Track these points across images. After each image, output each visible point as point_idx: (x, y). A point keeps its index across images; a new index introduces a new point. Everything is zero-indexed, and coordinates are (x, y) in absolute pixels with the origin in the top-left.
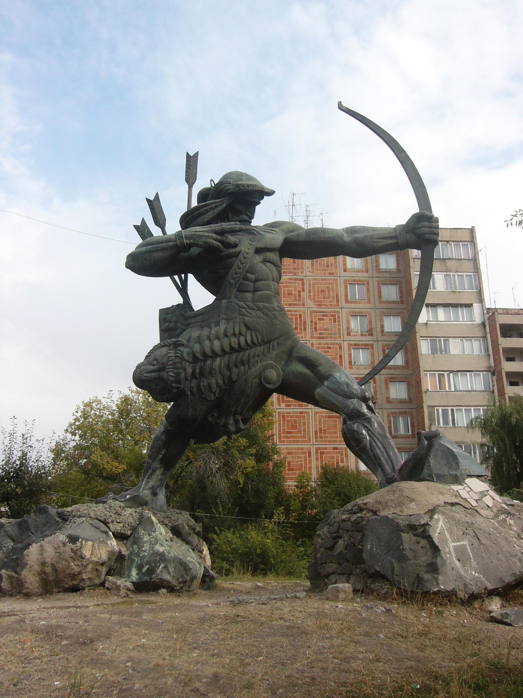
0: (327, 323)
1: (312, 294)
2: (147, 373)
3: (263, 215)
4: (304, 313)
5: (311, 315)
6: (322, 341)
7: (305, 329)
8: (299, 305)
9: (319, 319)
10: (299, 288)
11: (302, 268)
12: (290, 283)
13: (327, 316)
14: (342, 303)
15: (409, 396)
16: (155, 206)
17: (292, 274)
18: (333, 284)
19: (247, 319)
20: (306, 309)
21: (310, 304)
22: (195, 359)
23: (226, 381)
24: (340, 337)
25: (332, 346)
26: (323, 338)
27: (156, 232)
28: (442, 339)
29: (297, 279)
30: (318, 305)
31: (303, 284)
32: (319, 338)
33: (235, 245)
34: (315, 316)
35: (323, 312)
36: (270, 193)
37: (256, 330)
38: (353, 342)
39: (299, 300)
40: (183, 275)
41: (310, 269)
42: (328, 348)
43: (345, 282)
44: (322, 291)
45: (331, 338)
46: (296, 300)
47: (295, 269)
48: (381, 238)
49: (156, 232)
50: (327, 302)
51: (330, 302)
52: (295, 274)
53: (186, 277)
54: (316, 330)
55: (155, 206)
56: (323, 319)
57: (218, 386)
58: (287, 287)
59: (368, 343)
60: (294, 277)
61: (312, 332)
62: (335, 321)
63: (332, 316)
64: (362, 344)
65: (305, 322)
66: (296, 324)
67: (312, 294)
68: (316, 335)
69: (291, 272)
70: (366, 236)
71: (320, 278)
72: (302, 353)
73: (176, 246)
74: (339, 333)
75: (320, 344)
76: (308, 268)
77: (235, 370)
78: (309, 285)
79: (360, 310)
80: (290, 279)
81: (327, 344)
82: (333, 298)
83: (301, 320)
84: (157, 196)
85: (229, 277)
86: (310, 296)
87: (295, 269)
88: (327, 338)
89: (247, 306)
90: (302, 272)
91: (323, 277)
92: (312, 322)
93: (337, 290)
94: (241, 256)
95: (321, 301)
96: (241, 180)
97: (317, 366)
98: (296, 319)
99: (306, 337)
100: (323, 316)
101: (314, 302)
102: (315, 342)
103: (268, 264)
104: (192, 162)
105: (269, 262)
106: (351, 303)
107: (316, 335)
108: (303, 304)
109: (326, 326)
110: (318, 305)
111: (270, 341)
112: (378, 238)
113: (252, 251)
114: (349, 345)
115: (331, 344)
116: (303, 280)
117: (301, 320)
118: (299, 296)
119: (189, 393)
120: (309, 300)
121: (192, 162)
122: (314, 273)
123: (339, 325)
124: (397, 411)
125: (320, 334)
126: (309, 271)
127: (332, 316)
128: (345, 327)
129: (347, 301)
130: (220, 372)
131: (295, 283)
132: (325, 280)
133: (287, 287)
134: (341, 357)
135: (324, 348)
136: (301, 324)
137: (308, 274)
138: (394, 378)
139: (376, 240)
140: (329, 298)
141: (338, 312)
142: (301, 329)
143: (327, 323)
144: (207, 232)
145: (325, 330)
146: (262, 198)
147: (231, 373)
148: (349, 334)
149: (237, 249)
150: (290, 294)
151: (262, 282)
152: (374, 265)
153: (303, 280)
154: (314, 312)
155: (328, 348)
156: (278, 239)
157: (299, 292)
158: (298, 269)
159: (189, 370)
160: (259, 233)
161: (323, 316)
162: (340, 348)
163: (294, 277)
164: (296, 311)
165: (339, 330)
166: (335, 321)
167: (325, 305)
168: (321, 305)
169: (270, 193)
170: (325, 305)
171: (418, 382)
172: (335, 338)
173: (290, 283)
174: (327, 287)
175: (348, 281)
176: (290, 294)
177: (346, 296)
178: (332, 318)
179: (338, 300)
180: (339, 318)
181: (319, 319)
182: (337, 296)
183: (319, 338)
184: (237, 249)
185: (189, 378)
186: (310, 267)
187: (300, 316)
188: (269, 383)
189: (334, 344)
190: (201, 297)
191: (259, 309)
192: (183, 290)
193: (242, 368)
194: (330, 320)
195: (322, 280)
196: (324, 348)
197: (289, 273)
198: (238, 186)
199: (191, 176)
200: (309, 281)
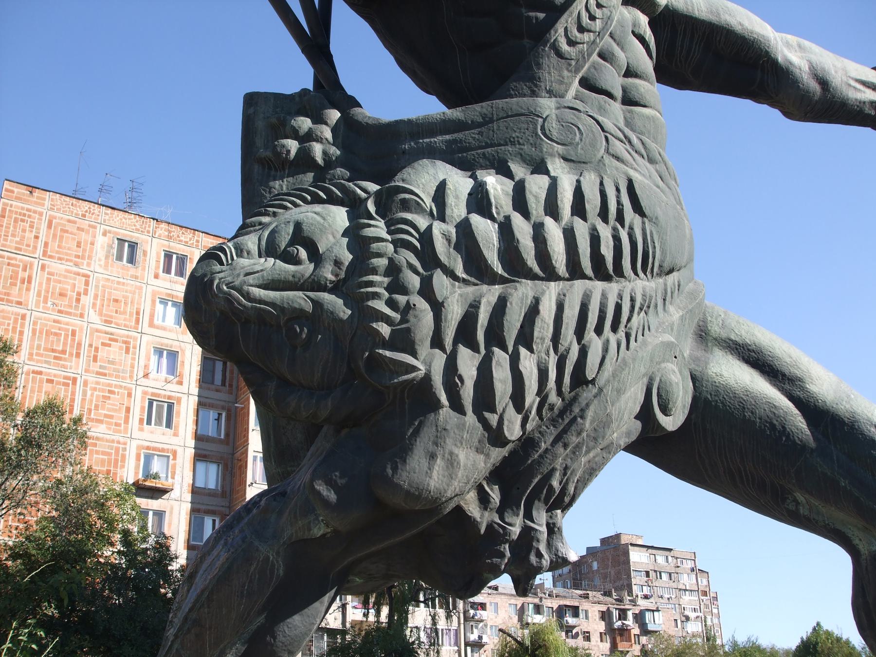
0: (114, 352)
1: (98, 302)
2: (265, 287)
4: (81, 329)
5: (91, 335)
6: (102, 380)
7: (78, 355)
8: (75, 315)
9: (103, 344)
10: (79, 287)
11: (90, 257)
12: (66, 277)
13: (116, 341)
15: (223, 487)
17: (71, 264)
18: (134, 293)
19: (635, 176)
20: (85, 324)
21: (94, 317)
23: (567, 379)
24: (131, 377)
25: (116, 390)
26: (105, 375)
29: (78, 274)
30: (106, 321)
31: (87, 283)
32: (98, 373)
34: (99, 338)
35: (111, 334)
37: (655, 221)
38: (150, 390)
39: (77, 307)
41: (102, 263)
42: (110, 392)
43: (154, 294)
44: (116, 301)
45: (117, 377)
46: (71, 306)
47: (78, 257)
50: (120, 319)
51: (125, 320)
52: (76, 265)
54: (95, 359)
56: (109, 345)
57: (539, 394)
58: (60, 282)
59: (173, 394)
60: (75, 269)
61: (88, 362)
62: (127, 351)
63: (125, 342)
64: (165, 396)
65: (79, 344)
66: (65, 344)
67: (98, 302)
68: (95, 367)
69: (71, 261)
71: (116, 279)
74: (132, 372)
75: (98, 383)
76: (100, 260)
77: (595, 344)
78: (97, 287)
79: (170, 342)
80: (67, 271)
81: (110, 385)
82: (131, 314)
83: (73, 340)
85: (558, 35)
86: (94, 305)
87: (78, 257)
88: (110, 375)
89: (626, 137)
90: (89, 265)
91: (121, 280)
92: (91, 345)
93: (139, 304)
95: (111, 317)
97: (800, 380)
98: (66, 336)
99: (77, 368)
100: (110, 339)
101: (101, 314)
102: (91, 378)
106: (158, 328)
107: (95, 367)
108: (82, 316)
109: (112, 357)
110: (106, 321)
111: (671, 271)
114: (145, 393)
115: (116, 386)
116: (88, 276)
117: (73, 340)
118: (78, 300)
119: (443, 398)
120: (92, 311)
122: (107, 270)
123: (133, 359)
124: (203, 507)
125: (101, 367)
126: (100, 266)
127: (125, 342)
128: (142, 364)
129: (151, 324)
130: (556, 339)
131: (75, 279)
132: (123, 284)
133: (60, 282)
134: (128, 410)
135: (103, 391)
136: (72, 346)
139: (853, 83)
140: (124, 313)
142: (71, 355)
143: (114, 352)
145: (112, 362)
147: (583, 353)
151: (647, 83)
153: (88, 276)
154: (97, 331)
157: (79, 294)
158: (83, 258)
161: (110, 339)
162: (129, 395)
163: (75, 269)
164: (67, 324)
165: (132, 367)
166: (127, 351)
167: (116, 324)
168: (111, 322)
170: (116, 324)
171: (240, 467)
172: (123, 378)
173: (66, 277)
174: (123, 297)
175: (159, 293)
177: (152, 316)
178: (124, 346)
179: (137, 320)
180: (135, 348)
181: (103, 344)
182: (138, 313)
183: (98, 373)
186: (103, 259)
187: (74, 333)
188: (665, 411)
189: (121, 387)
191: (651, 161)
193: (613, 338)
194: (121, 348)
195: (118, 283)
196: (103, 391)
197: (67, 260)
200: (98, 281)
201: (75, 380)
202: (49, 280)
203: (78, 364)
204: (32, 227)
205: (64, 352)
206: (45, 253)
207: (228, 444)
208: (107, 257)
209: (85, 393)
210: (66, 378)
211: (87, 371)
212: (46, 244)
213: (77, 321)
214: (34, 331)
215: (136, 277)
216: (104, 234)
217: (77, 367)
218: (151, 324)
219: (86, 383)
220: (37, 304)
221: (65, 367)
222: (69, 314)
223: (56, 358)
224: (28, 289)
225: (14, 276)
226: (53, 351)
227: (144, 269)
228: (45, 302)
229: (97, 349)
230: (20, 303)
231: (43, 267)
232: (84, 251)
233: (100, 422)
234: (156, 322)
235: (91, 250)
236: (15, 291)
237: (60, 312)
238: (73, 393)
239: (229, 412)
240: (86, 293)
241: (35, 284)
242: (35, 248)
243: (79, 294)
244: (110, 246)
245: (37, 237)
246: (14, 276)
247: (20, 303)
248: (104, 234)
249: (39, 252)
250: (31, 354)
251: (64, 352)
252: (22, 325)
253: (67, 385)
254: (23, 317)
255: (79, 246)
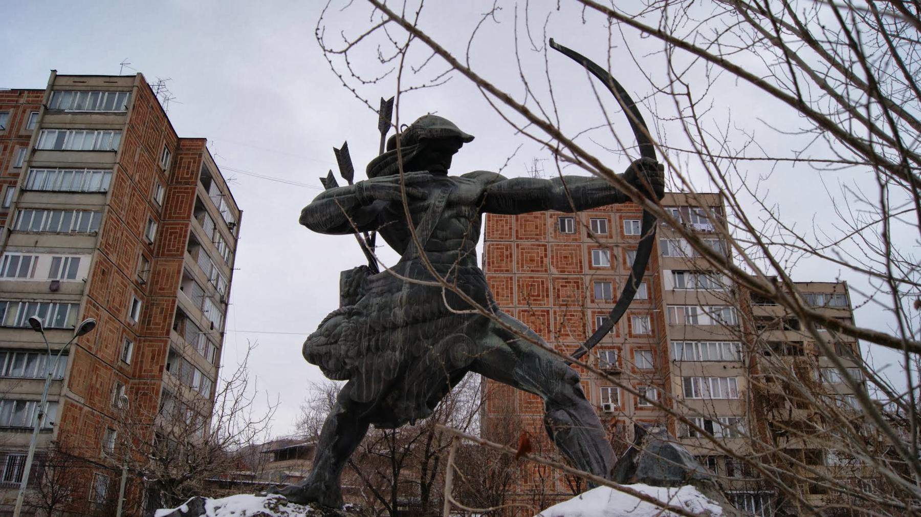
3: (461, 164)
5: (554, 282)
7: (548, 296)
11: (545, 234)
14: (586, 269)
16: (343, 155)
21: (554, 270)
22: (372, 331)
27: (342, 183)
28: (690, 307)
29: (539, 245)
31: (546, 250)
33: (424, 198)
36: (470, 139)
39: (542, 266)
40: (370, 233)
44: (565, 257)
46: (538, 266)
47: (537, 235)
48: (596, 189)
49: (342, 183)
50: (570, 268)
52: (537, 240)
53: (374, 236)
54: (558, 297)
55: (343, 155)
61: (555, 301)
62: (578, 288)
65: (547, 289)
70: (578, 188)
72: (498, 326)
73: (356, 198)
80: (534, 245)
84: (345, 146)
86: (552, 262)
87: (537, 235)
90: (545, 238)
92: (554, 289)
93: (580, 256)
94: (429, 211)
96: (434, 124)
98: (538, 285)
103: (463, 220)
104: (387, 109)
105: (465, 217)
108: (546, 271)
112: (592, 190)
113: (443, 204)
114: (593, 313)
118: (542, 262)
121: (387, 109)
129: (591, 268)
137: (551, 240)
138: (640, 347)
141: (582, 279)
142: (543, 296)
144: (391, 182)
145: (568, 297)
146: (461, 146)
148: (593, 301)
149: (426, 203)
150: (532, 260)
152: (619, 230)
154: (558, 278)
155: (571, 315)
156: (472, 190)
157: (542, 258)
159: (365, 344)
160: (453, 184)
166: (578, 288)
169: (470, 139)
176: (532, 260)
177: (590, 262)
182: (581, 262)
184: (426, 203)
185: (364, 351)
187: (543, 282)
190: (388, 256)
192: (368, 247)
198: (430, 131)
199: (384, 125)
201: (548, 312)
202: (522, 253)
203: (548, 301)
204: (506, 223)
205: (538, 296)
206: (517, 236)
207: (654, 337)
208: (555, 231)
209: (555, 319)
210: (542, 311)
211: (554, 305)
212: (517, 231)
213: (544, 275)
214: (519, 286)
215: (576, 240)
216: (551, 217)
217: (549, 303)
218: (591, 268)
219: (555, 313)
220: (518, 270)
221: (540, 304)
222: (538, 271)
223: (535, 300)
224: (511, 261)
225: (502, 256)
226: (533, 296)
227: (580, 233)
228: (522, 267)
229: (558, 290)
230: (507, 271)
231: (518, 246)
232: (541, 230)
233: (568, 335)
234: (594, 265)
235: (545, 229)
236: (504, 264)
237: (532, 271)
238: (548, 320)
239: (652, 315)
240: (546, 256)
241: (514, 257)
242: (511, 235)
243: (542, 258)
244: (556, 224)
245: (511, 228)
246: (502, 256)
247: (507, 271)
248: (551, 217)
249: (514, 238)
250: (519, 301)
251: (538, 296)
252: (511, 283)
253: (543, 315)
254: (511, 279)
255: (537, 228)
